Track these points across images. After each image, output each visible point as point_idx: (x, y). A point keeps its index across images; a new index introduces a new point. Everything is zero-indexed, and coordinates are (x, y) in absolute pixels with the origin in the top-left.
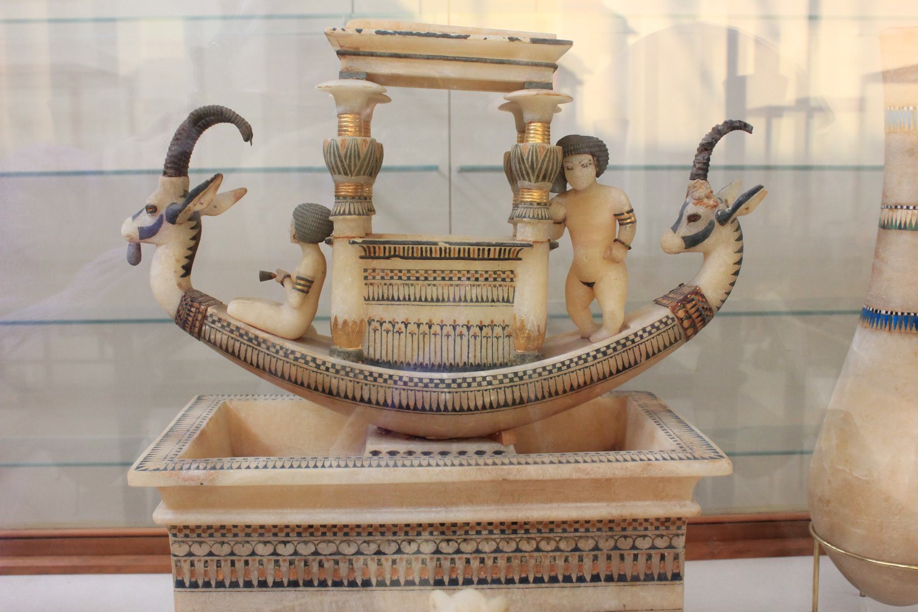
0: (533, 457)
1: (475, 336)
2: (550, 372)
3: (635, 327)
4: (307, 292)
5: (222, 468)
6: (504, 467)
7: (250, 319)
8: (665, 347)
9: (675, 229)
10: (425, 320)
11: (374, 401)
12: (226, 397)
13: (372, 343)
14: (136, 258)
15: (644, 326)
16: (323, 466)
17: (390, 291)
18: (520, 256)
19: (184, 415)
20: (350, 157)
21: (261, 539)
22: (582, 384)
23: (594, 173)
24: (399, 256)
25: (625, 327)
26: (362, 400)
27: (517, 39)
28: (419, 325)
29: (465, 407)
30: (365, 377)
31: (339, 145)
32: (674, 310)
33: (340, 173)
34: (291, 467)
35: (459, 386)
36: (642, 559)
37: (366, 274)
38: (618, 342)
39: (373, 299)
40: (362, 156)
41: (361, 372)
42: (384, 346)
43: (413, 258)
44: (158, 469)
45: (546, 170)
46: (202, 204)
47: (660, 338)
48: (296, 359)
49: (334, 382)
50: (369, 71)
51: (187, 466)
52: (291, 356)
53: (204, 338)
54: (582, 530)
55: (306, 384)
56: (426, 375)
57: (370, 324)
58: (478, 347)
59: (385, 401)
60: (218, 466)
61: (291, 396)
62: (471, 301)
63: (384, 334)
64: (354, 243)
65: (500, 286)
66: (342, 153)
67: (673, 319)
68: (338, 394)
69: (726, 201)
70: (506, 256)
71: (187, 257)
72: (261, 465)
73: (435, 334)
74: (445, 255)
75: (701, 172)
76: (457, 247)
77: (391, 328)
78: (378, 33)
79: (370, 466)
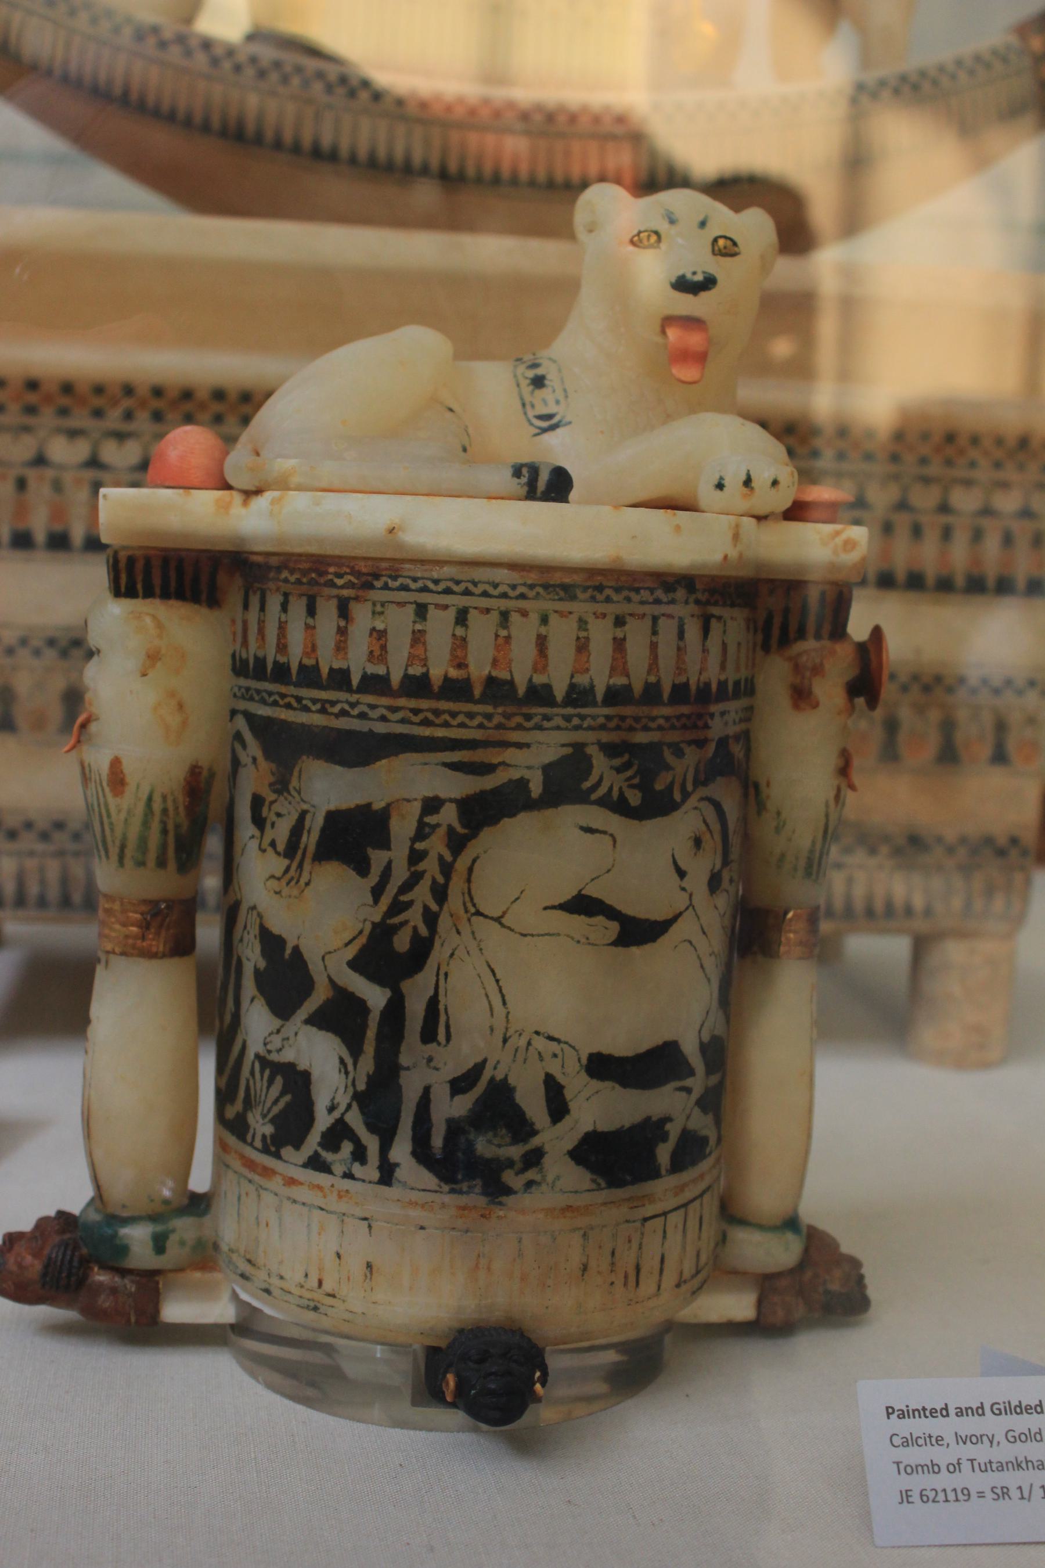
49: (253, 101)
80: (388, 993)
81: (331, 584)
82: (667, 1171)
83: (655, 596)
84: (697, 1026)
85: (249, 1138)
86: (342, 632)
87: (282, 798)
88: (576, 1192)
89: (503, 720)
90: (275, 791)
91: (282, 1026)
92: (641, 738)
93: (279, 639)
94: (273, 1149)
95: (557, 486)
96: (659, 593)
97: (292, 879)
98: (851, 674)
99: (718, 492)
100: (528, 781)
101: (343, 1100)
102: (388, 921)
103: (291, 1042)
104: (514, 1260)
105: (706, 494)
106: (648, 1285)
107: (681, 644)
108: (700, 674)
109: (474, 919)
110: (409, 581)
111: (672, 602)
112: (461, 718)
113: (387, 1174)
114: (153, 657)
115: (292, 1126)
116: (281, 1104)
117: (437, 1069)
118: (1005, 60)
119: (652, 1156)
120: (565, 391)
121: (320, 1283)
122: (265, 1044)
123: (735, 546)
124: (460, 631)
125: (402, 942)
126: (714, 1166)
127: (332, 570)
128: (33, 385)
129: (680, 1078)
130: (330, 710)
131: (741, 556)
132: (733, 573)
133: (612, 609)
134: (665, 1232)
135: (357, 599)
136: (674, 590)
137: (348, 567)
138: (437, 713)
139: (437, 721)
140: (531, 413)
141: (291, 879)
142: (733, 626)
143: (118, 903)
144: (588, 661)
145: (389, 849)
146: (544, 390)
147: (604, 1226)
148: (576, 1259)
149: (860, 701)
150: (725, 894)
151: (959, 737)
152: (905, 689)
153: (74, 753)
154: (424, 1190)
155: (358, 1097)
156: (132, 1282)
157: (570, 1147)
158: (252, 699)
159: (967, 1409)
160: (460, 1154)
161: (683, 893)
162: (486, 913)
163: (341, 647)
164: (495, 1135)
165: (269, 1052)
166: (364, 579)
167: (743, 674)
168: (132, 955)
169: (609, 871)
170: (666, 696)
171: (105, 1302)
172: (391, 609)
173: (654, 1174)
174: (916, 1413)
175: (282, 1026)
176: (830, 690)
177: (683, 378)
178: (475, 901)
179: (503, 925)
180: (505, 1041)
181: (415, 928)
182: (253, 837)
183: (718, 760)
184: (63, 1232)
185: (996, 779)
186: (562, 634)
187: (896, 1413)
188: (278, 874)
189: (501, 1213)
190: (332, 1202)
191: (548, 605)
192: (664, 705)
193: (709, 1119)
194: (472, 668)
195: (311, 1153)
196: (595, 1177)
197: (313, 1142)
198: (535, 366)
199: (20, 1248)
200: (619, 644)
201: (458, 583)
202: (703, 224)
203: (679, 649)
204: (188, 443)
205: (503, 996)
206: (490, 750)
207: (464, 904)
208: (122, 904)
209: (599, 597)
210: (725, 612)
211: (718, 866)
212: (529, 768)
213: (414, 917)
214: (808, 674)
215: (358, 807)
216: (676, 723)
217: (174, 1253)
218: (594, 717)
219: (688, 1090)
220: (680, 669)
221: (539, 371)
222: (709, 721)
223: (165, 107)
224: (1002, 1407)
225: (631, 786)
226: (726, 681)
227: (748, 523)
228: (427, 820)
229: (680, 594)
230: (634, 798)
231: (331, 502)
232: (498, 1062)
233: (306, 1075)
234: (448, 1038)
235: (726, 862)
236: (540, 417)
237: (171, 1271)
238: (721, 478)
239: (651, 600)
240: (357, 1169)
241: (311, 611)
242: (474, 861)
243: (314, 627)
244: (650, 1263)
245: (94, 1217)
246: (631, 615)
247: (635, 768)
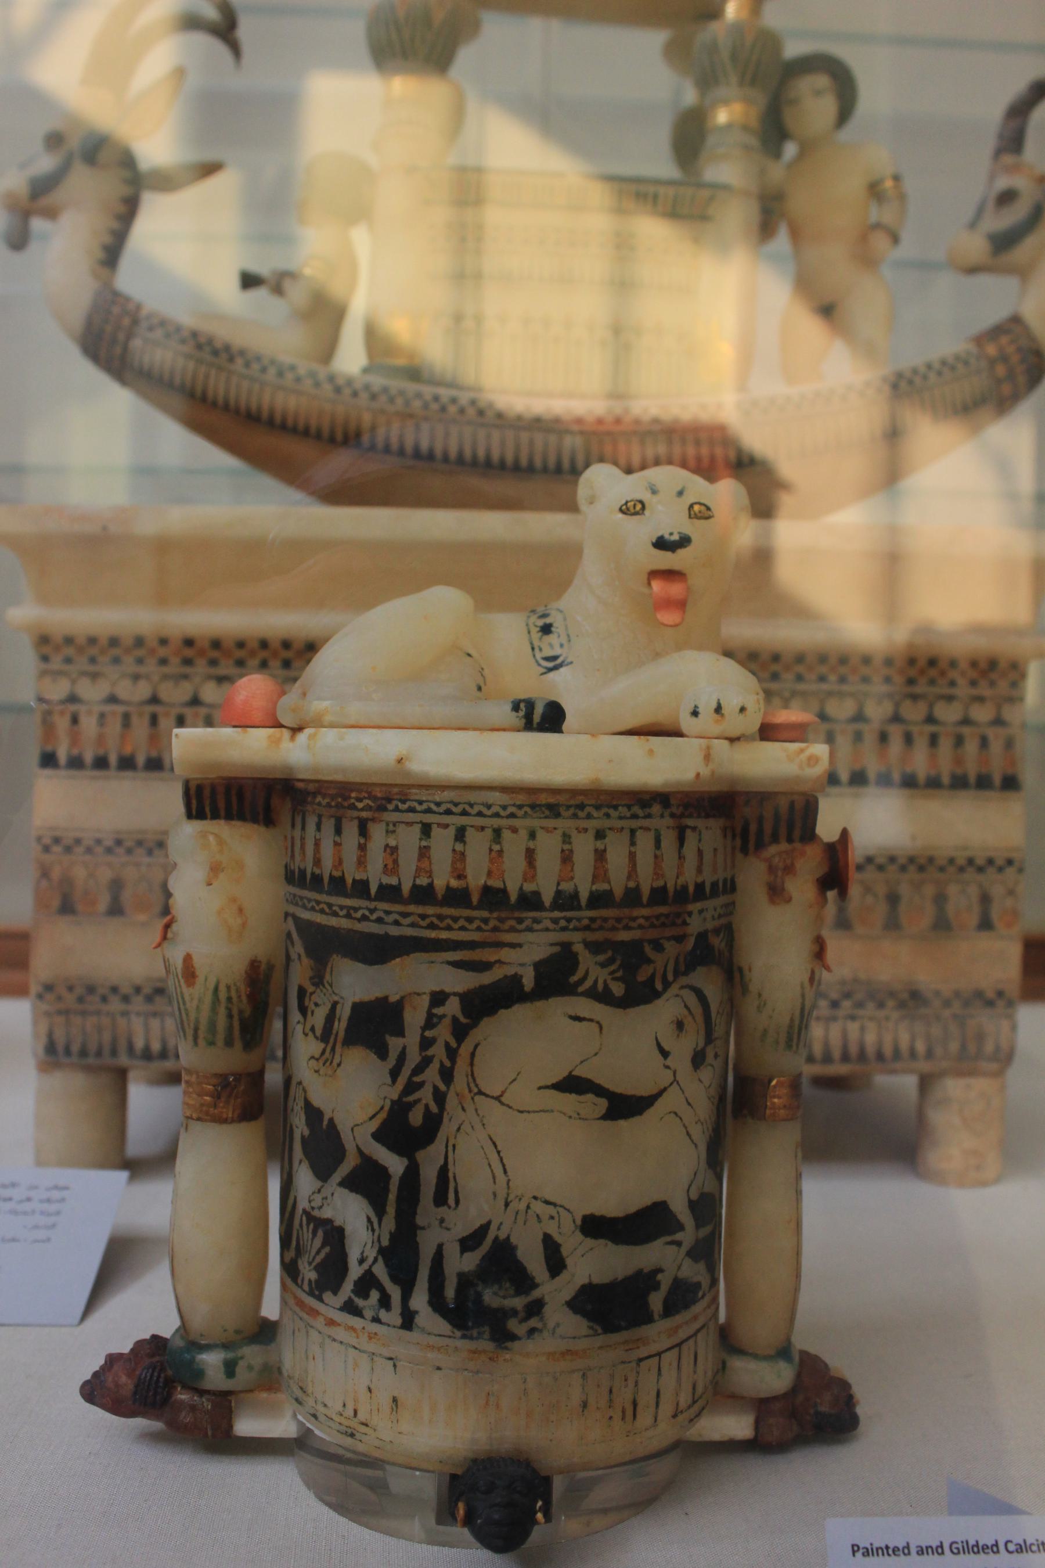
9: (973, 225)
21: (214, 671)
36: (945, 745)
54: (833, 678)
80: (405, 1162)
81: (353, 807)
82: (660, 1316)
83: (632, 812)
84: (686, 1187)
85: (299, 1282)
86: (362, 848)
87: (318, 990)
88: (574, 1338)
89: (497, 924)
90: (314, 984)
91: (322, 1187)
92: (624, 936)
93: (315, 855)
94: (317, 1293)
95: (552, 719)
96: (636, 809)
97: (327, 1060)
98: (820, 873)
99: (694, 719)
100: (521, 976)
101: (371, 1254)
102: (404, 1099)
103: (329, 1201)
104: (520, 1399)
105: (686, 723)
106: (645, 1418)
107: (658, 853)
108: (678, 877)
109: (477, 1098)
110: (416, 804)
111: (649, 816)
112: (461, 922)
113: (408, 1321)
114: (215, 869)
115: (332, 1272)
116: (322, 1255)
117: (448, 1229)
118: (966, 363)
119: (646, 1305)
120: (568, 636)
121: (355, 1412)
122: (310, 1202)
123: (707, 765)
124: (459, 847)
125: (416, 1118)
126: (709, 1307)
127: (353, 795)
128: (189, 642)
129: (670, 1233)
130: (354, 915)
131: (713, 773)
132: (706, 789)
133: (592, 824)
134: (659, 1370)
135: (373, 820)
136: (650, 806)
137: (367, 792)
138: (441, 917)
139: (441, 925)
140: (539, 656)
141: (326, 1060)
142: (709, 834)
143: (194, 1076)
144: (572, 870)
145: (404, 1036)
146: (551, 635)
147: (602, 1367)
148: (576, 1397)
149: (831, 895)
150: (710, 1068)
151: (950, 909)
152: (903, 868)
153: (159, 949)
154: (440, 1335)
155: (382, 1251)
156: (208, 1400)
157: (568, 1298)
158: (297, 904)
159: (927, 1548)
160: (470, 1304)
161: (668, 1071)
162: (488, 1092)
163: (361, 862)
164: (500, 1288)
165: (313, 1208)
166: (379, 803)
167: (720, 875)
168: (206, 1121)
169: (596, 1054)
170: (645, 899)
171: (186, 1418)
172: (401, 829)
173: (649, 1319)
174: (880, 1551)
175: (322, 1187)
176: (802, 887)
177: (666, 622)
178: (478, 1081)
179: (502, 1104)
180: (507, 1205)
181: (427, 1106)
182: (299, 1022)
183: (698, 952)
184: (153, 1355)
185: (985, 942)
186: (548, 846)
187: (861, 1551)
188: (317, 1056)
189: (508, 1356)
190: (363, 1342)
191: (535, 823)
192: (644, 906)
193: (701, 1266)
194: (470, 878)
195: (346, 1299)
196: (591, 1324)
197: (347, 1288)
198: (544, 616)
199: (116, 1367)
200: (600, 855)
201: (456, 805)
202: (680, 493)
203: (656, 857)
204: (253, 687)
205: (504, 1166)
206: (487, 950)
207: (468, 1085)
208: (198, 1076)
209: (581, 814)
210: (699, 823)
211: (701, 1044)
212: (522, 965)
213: (426, 1095)
214: (780, 873)
215: (377, 999)
216: (655, 922)
217: (244, 1376)
218: (579, 920)
219: (679, 1244)
220: (658, 873)
221: (548, 621)
222: (688, 920)
223: (301, 426)
224: (960, 1546)
225: (614, 979)
226: (703, 883)
227: (721, 747)
228: (435, 1011)
229: (656, 809)
230: (618, 989)
231: (353, 737)
232: (501, 1224)
233: (340, 1232)
234: (457, 1201)
235: (709, 1039)
236: (547, 659)
237: (241, 1392)
238: (696, 707)
239: (628, 815)
240: (383, 1314)
241: (338, 831)
242: (476, 1046)
243: (340, 844)
244: (646, 1399)
245: (179, 1343)
246: (610, 829)
247: (618, 962)
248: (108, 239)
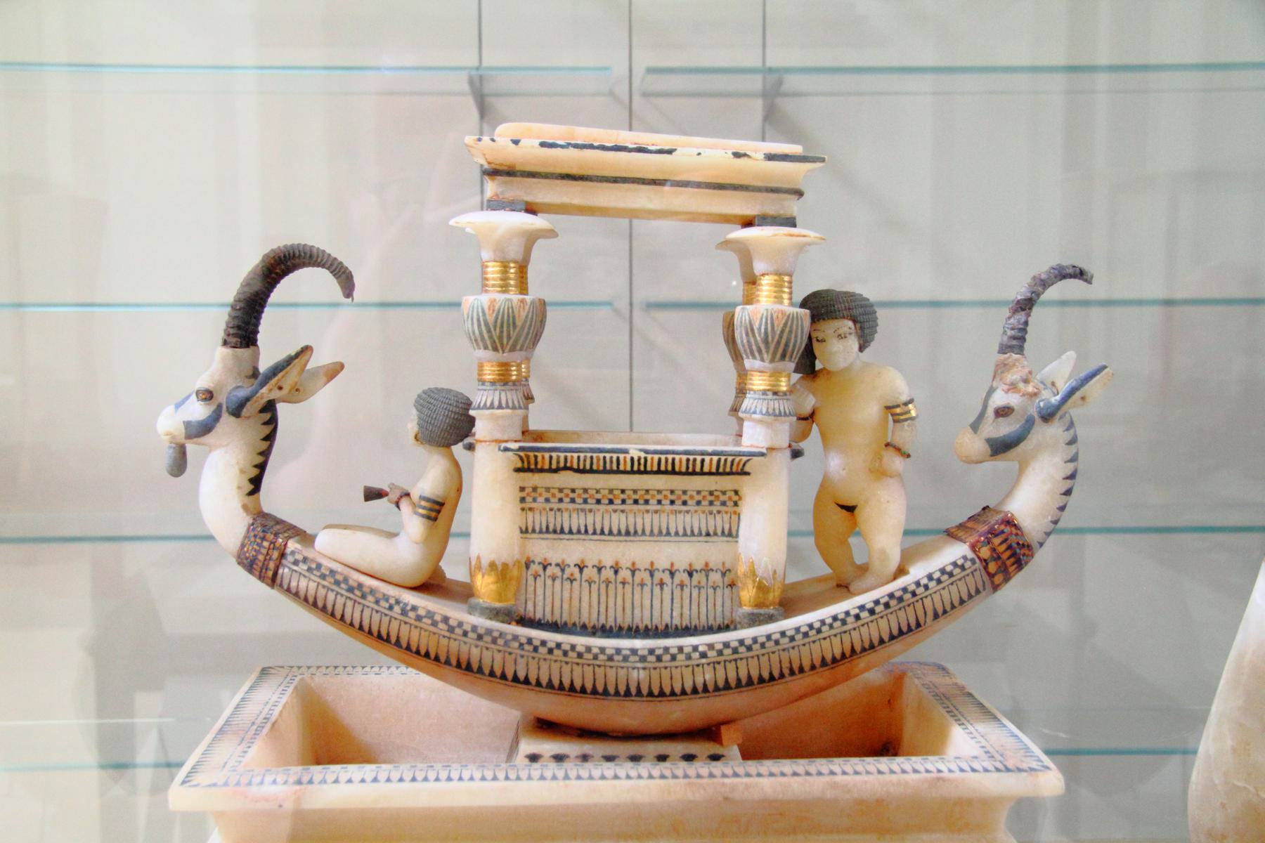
0: (768, 765)
1: (682, 586)
2: (792, 639)
3: (918, 572)
4: (435, 519)
5: (311, 782)
6: (727, 781)
7: (351, 557)
8: (962, 602)
9: (975, 427)
10: (608, 562)
11: (533, 681)
12: (304, 670)
13: (530, 595)
14: (179, 464)
15: (931, 571)
16: (461, 779)
17: (559, 519)
18: (747, 469)
19: (243, 699)
20: (502, 326)
22: (838, 656)
23: (856, 346)
24: (571, 469)
25: (901, 571)
26: (516, 679)
27: (745, 155)
28: (599, 570)
29: (667, 690)
30: (521, 645)
31: (486, 307)
32: (973, 547)
33: (486, 348)
34: (414, 779)
35: (659, 659)
37: (523, 494)
38: (891, 596)
39: (534, 531)
40: (519, 323)
41: (516, 638)
42: (549, 600)
43: (591, 471)
44: (215, 785)
45: (787, 345)
46: (280, 388)
47: (953, 588)
48: (419, 618)
49: (475, 653)
50: (529, 199)
51: (258, 779)
52: (412, 614)
53: (281, 585)
55: (433, 656)
56: (610, 643)
57: (527, 567)
58: (687, 602)
59: (550, 680)
60: (305, 779)
61: (403, 669)
62: (677, 534)
63: (549, 582)
64: (507, 449)
65: (719, 512)
66: (491, 319)
67: (973, 561)
68: (480, 670)
69: (1053, 384)
70: (728, 470)
71: (256, 466)
72: (369, 778)
73: (624, 583)
74: (639, 469)
75: (1014, 342)
76: (656, 457)
77: (559, 574)
78: (543, 145)
79: (530, 778)
248: (255, 472)
